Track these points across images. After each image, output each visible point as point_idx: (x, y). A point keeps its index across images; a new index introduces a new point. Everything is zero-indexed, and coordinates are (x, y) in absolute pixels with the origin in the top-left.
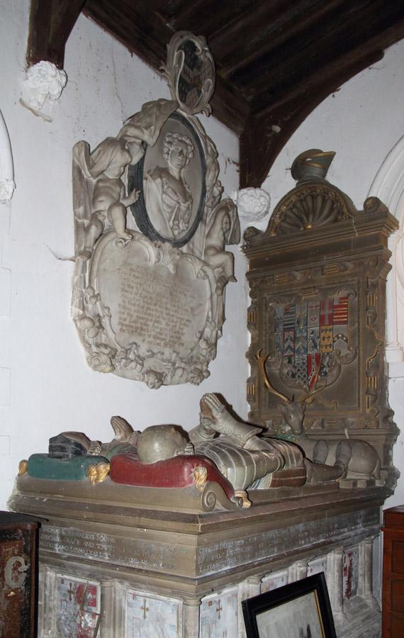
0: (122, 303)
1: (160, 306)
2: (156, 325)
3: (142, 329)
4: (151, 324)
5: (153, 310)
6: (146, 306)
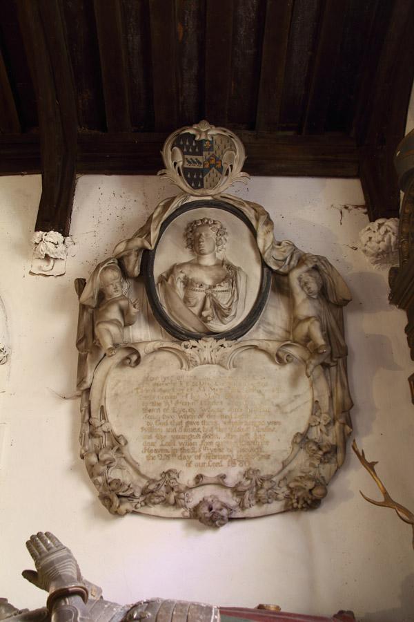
0: (146, 426)
1: (209, 416)
2: (207, 440)
3: (182, 450)
4: (199, 441)
5: (198, 423)
6: (185, 421)
